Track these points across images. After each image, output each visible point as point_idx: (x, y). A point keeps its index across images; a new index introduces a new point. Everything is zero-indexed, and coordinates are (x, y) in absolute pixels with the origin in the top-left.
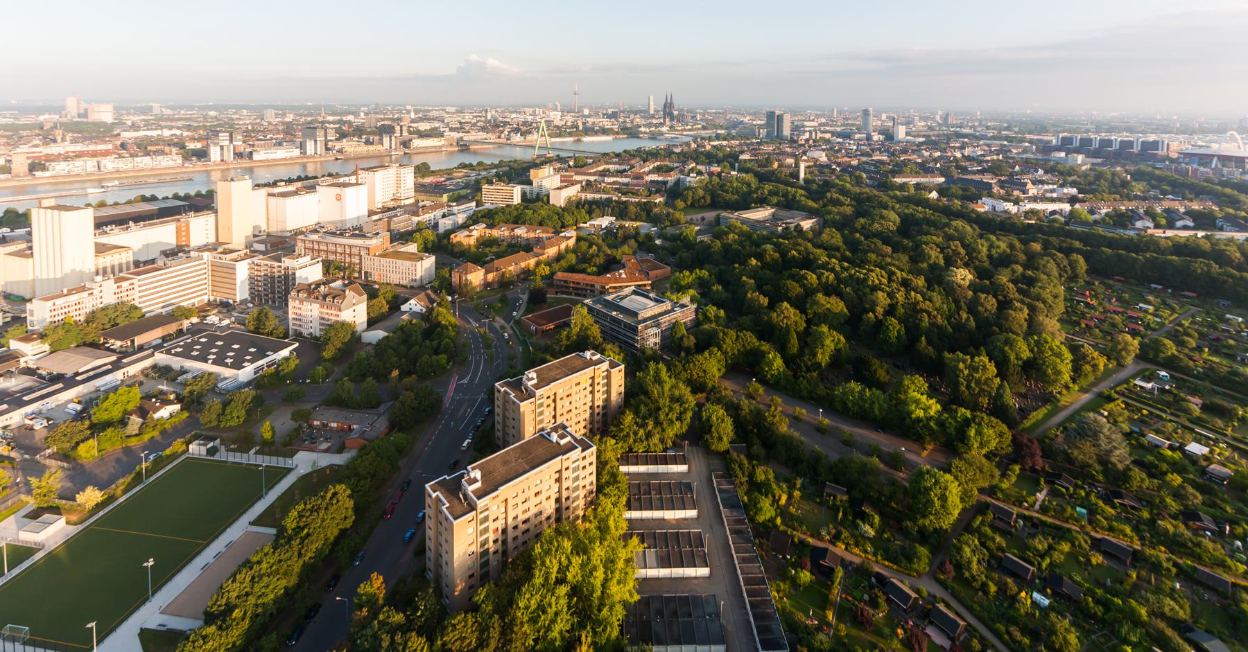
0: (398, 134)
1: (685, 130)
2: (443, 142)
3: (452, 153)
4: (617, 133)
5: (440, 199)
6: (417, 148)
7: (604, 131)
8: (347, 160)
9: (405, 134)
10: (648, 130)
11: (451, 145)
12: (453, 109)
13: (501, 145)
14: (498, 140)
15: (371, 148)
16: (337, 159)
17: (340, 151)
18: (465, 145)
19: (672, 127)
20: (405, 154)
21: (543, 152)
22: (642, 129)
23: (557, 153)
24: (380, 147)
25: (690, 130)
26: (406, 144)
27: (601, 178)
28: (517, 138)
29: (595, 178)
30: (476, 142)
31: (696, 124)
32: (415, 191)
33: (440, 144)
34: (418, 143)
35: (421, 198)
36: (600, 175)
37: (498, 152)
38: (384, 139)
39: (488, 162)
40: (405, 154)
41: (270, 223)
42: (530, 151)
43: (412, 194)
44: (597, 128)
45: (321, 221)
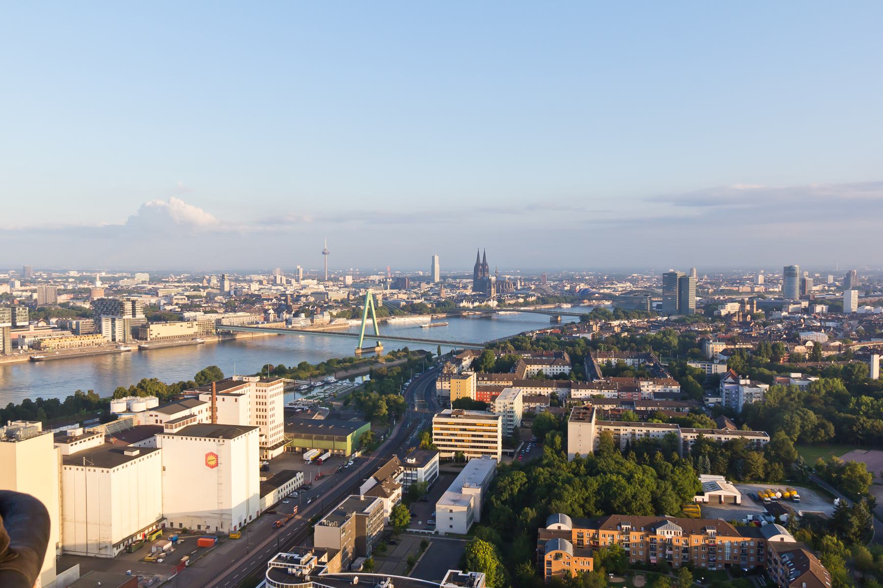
0: (128, 316)
1: (521, 305)
2: (196, 329)
3: (208, 347)
4: (433, 311)
5: (339, 445)
6: (157, 339)
7: (414, 309)
8: (50, 361)
9: (140, 316)
10: (471, 306)
11: (208, 333)
12: (146, 277)
13: (281, 333)
14: (266, 325)
15: (88, 340)
16: (32, 360)
17: (36, 346)
18: (228, 333)
19: (500, 301)
20: (141, 349)
21: (371, 343)
22: (464, 304)
23: (400, 346)
24: (99, 339)
25: (526, 304)
26: (138, 333)
27: (560, 392)
28: (302, 321)
29: (550, 390)
30: (243, 328)
31: (528, 296)
32: (287, 429)
33: (191, 331)
34: (157, 330)
35: (299, 443)
36: (559, 386)
37: (282, 344)
38: (104, 324)
39: (313, 362)
40: (141, 349)
41: (66, 524)
42: (351, 341)
43: (281, 436)
44: (403, 303)
45: (167, 512)
